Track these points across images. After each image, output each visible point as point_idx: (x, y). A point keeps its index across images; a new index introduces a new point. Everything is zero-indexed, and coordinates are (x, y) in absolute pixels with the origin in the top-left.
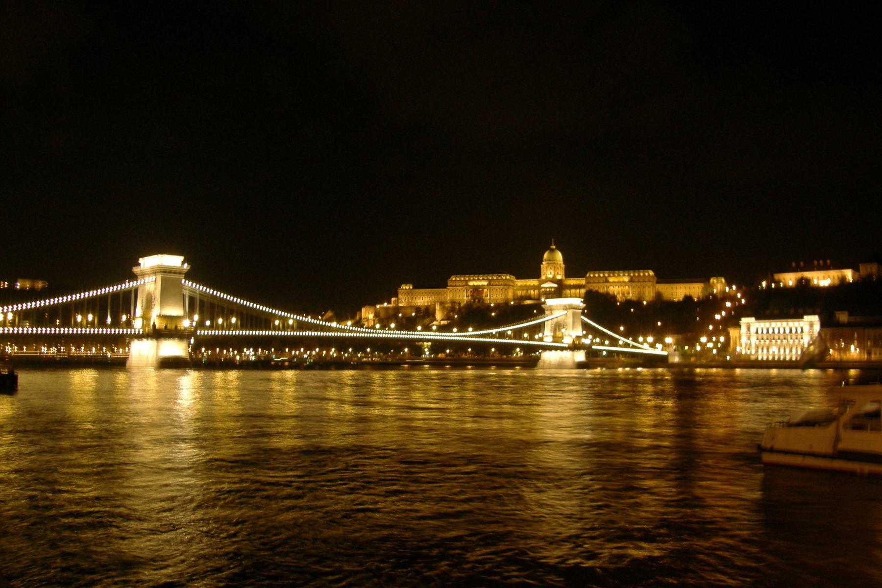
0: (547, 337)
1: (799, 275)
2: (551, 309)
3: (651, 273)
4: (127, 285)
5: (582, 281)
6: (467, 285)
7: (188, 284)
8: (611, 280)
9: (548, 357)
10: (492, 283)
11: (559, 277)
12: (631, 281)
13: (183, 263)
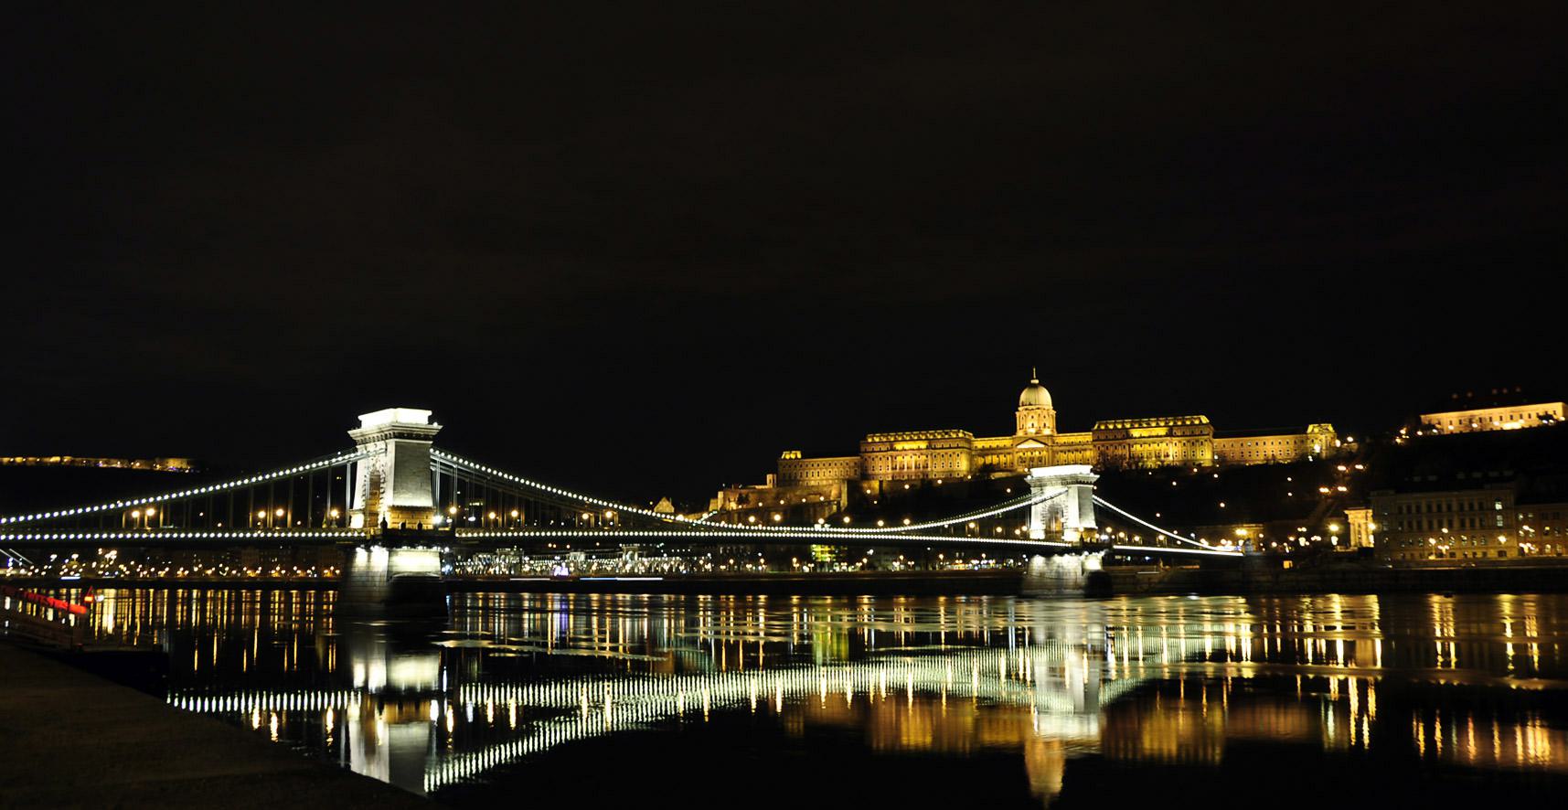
0: (1036, 530)
2: (1041, 484)
3: (1205, 420)
4: (339, 460)
5: (1086, 437)
6: (893, 449)
7: (438, 455)
8: (1136, 433)
11: (1047, 432)
12: (1170, 434)
13: (431, 420)
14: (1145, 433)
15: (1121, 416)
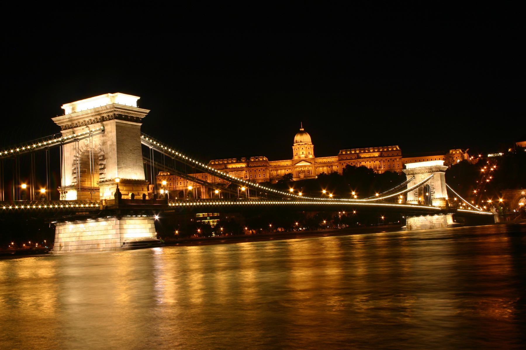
2: (413, 174)
3: (398, 149)
4: (54, 142)
6: (226, 168)
9: (416, 222)
10: (250, 165)
12: (381, 156)
13: (140, 104)
14: (367, 155)
15: (355, 147)
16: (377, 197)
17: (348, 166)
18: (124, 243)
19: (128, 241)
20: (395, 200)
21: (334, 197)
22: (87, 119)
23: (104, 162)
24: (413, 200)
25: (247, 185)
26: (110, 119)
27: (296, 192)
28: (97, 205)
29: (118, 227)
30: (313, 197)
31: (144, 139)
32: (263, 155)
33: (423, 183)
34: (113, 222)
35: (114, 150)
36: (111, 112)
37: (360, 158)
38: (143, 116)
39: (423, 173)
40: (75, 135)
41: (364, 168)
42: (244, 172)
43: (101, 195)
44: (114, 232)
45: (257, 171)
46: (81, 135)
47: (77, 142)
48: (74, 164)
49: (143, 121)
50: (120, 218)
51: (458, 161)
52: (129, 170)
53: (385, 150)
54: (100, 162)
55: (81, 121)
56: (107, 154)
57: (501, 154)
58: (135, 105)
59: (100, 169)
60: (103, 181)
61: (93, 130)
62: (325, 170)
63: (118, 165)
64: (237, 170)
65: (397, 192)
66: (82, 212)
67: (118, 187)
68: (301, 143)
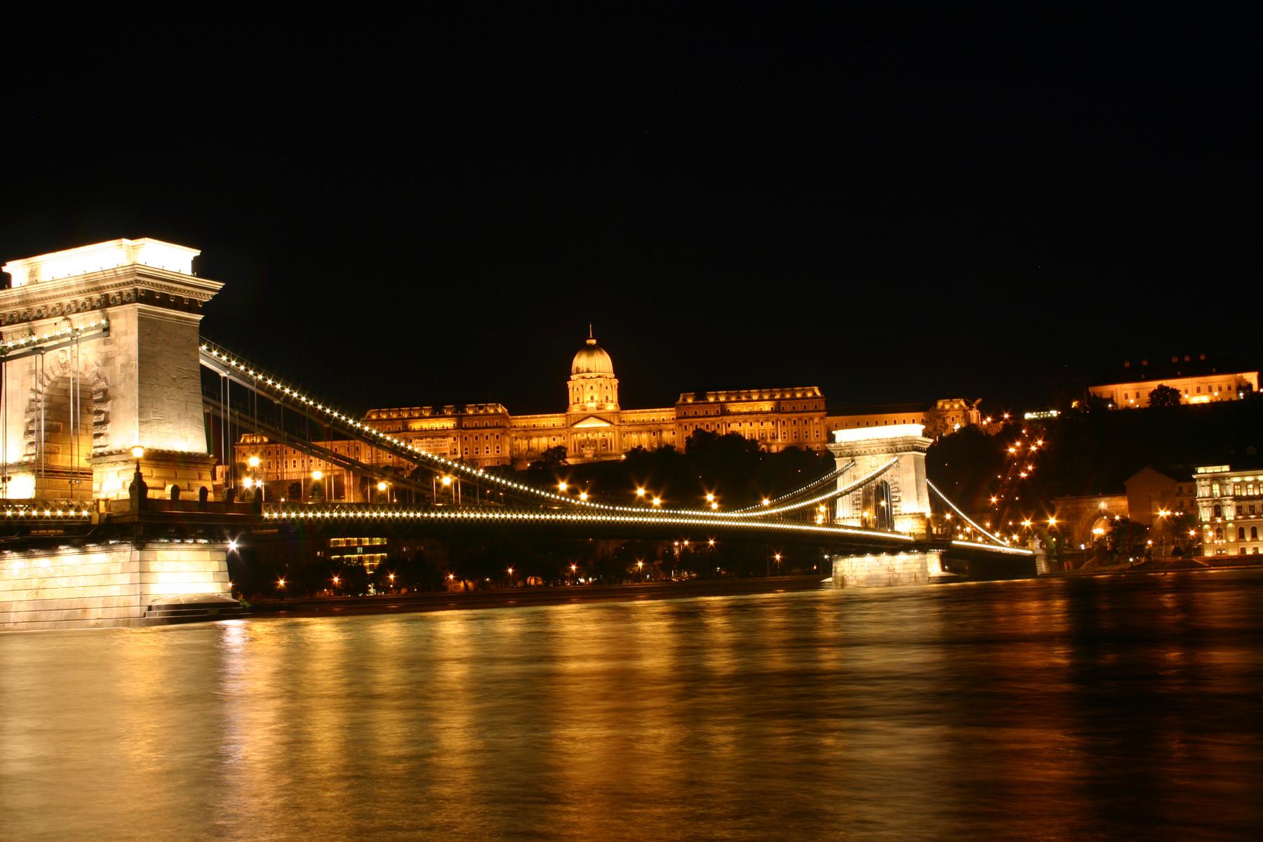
1: (1154, 385)
3: (818, 394)
6: (406, 429)
10: (465, 423)
12: (776, 410)
13: (200, 267)
15: (716, 388)
16: (766, 508)
17: (698, 432)
18: (150, 608)
19: (159, 603)
20: (806, 515)
21: (664, 506)
22: (66, 301)
23: (106, 408)
24: (850, 517)
25: (457, 472)
26: (123, 303)
27: (573, 492)
28: (85, 513)
29: (136, 566)
30: (615, 503)
31: (208, 353)
32: (497, 400)
33: (873, 478)
34: (125, 554)
35: (132, 377)
36: (128, 283)
37: (725, 413)
38: (207, 297)
39: (873, 453)
40: (35, 339)
41: (736, 438)
42: (451, 440)
43: (95, 487)
44: (126, 578)
45: (481, 439)
46: (51, 339)
47: (39, 356)
48: (30, 410)
49: (205, 308)
50: (141, 544)
51: (957, 427)
52: (166, 428)
53: (788, 396)
54: (96, 407)
55: (52, 304)
56: (114, 386)
57: (1054, 413)
58: (187, 269)
59: (97, 424)
60: (102, 455)
61: (81, 327)
62: (644, 440)
63: (141, 414)
64: (432, 436)
65: (811, 497)
66: (47, 528)
67: (138, 469)
68: (588, 375)
